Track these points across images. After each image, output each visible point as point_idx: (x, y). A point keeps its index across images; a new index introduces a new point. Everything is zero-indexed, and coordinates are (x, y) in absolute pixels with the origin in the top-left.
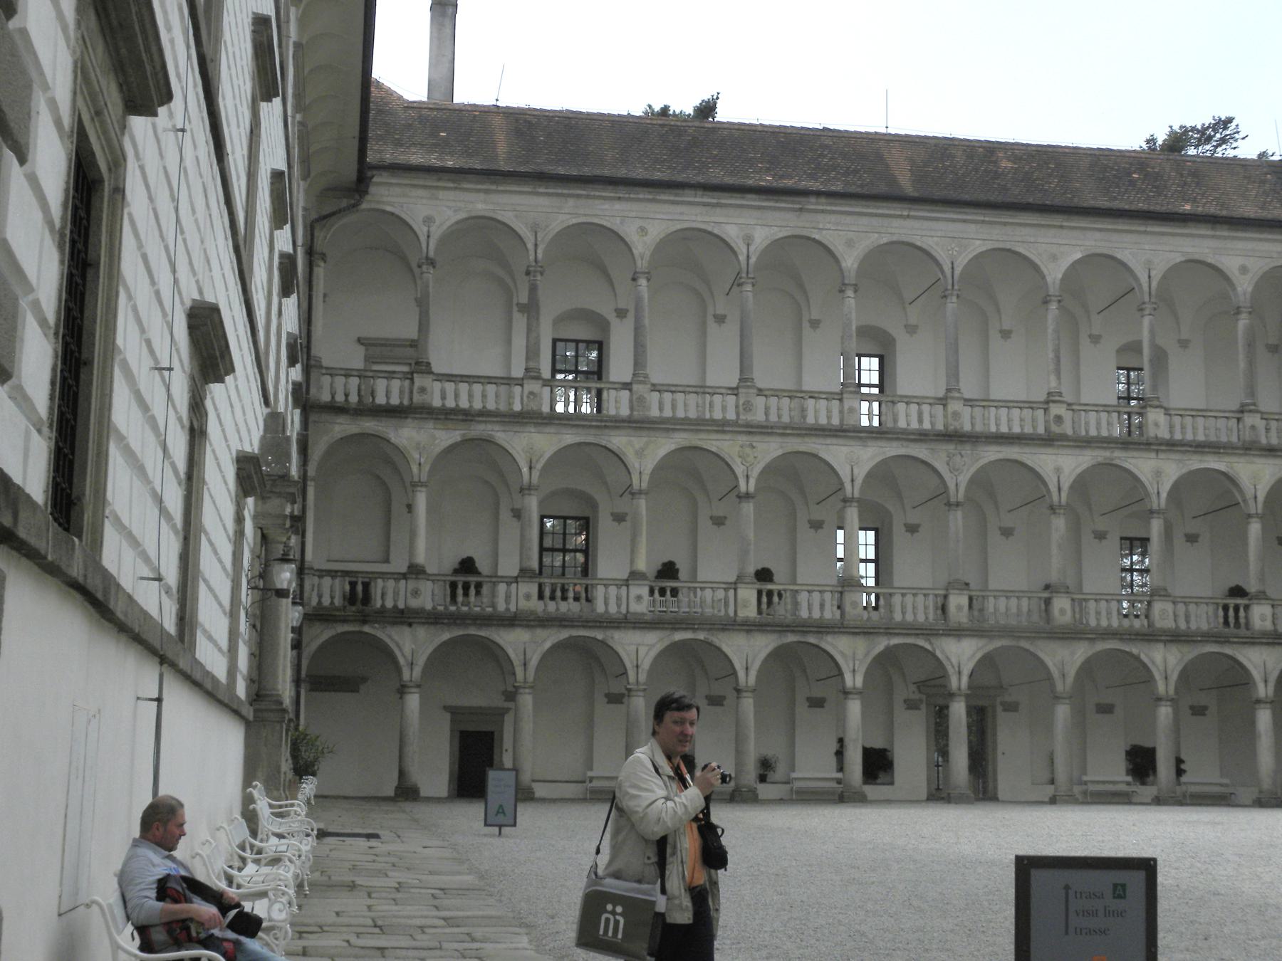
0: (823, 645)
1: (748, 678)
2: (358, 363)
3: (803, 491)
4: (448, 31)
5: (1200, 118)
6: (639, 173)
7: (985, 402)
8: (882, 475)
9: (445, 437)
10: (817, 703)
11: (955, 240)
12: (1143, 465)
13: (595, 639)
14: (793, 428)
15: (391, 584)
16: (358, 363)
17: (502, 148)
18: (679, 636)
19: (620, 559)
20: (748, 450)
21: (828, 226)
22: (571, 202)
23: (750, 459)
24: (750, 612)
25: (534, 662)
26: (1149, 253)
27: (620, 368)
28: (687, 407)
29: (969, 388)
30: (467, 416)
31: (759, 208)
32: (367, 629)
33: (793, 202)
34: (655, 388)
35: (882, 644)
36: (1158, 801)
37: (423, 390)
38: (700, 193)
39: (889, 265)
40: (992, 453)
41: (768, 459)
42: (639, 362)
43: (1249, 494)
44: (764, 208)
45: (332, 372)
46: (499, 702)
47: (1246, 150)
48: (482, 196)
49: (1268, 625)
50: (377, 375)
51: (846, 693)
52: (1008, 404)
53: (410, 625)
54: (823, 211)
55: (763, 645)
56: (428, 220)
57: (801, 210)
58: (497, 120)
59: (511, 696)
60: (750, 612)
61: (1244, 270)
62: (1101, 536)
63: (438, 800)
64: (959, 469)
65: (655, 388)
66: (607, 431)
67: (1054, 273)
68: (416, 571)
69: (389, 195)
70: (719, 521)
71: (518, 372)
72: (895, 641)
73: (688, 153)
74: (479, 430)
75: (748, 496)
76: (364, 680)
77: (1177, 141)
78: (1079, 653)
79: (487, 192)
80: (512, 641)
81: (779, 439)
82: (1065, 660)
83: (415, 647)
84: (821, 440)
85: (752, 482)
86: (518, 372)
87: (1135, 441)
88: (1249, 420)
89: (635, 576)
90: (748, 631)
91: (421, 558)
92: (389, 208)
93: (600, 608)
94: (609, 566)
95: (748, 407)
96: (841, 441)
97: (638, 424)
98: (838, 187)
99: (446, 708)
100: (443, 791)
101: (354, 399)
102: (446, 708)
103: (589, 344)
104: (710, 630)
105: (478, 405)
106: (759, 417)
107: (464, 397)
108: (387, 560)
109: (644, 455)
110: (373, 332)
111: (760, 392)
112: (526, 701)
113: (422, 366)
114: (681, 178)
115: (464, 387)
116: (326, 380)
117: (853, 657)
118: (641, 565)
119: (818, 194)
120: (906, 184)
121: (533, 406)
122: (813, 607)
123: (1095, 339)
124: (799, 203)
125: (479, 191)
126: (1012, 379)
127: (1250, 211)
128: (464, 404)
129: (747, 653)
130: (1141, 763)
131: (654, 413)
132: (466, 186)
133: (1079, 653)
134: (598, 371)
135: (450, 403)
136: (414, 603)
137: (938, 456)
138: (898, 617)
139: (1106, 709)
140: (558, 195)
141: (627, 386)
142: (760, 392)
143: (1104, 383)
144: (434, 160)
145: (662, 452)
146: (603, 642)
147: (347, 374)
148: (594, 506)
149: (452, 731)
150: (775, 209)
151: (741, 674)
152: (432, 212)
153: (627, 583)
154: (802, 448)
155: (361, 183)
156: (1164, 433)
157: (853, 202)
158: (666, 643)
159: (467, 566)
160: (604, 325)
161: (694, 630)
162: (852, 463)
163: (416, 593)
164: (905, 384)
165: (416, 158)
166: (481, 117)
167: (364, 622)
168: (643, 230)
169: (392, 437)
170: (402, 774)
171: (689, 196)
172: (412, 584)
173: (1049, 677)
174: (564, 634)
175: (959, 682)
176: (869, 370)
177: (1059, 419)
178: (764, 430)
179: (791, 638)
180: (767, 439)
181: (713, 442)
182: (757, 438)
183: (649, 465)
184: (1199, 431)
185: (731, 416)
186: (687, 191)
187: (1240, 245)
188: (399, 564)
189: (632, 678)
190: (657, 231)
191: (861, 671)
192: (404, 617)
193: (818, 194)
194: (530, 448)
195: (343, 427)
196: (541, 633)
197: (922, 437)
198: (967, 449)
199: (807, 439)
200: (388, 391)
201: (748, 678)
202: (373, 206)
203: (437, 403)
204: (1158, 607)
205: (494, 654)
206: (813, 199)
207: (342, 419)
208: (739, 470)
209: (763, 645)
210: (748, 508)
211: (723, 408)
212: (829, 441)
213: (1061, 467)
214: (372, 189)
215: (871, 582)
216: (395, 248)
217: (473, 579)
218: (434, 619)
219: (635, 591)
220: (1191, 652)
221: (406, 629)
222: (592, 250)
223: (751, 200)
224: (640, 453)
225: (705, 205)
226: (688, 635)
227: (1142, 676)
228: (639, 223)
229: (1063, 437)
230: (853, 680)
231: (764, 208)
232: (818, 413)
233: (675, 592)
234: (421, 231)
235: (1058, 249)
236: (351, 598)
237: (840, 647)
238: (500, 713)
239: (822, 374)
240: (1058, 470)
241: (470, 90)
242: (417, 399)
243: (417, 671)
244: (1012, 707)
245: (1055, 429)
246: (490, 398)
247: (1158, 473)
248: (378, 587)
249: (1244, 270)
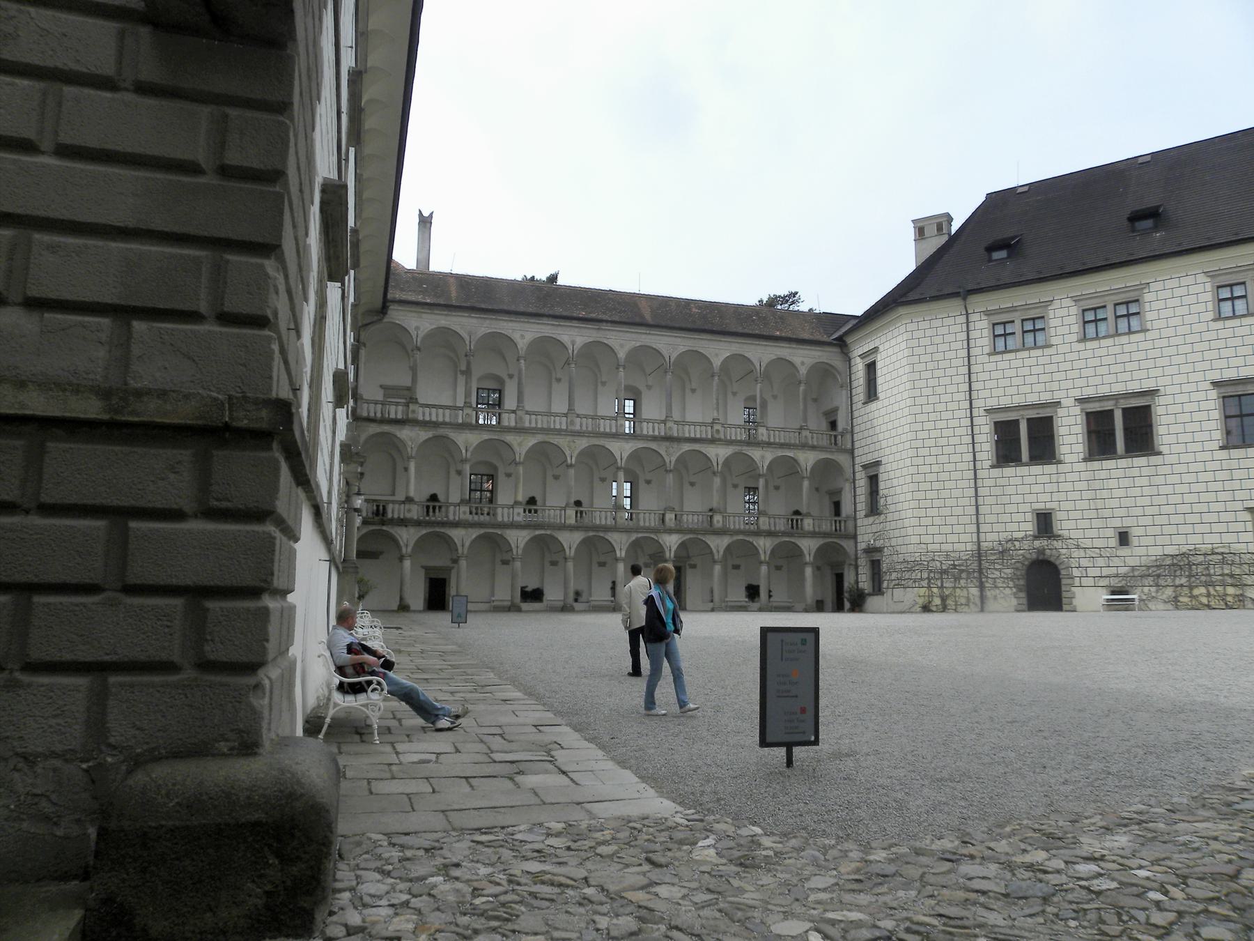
1: (570, 552)
2: (380, 397)
3: (597, 463)
5: (783, 292)
6: (521, 308)
7: (682, 423)
8: (635, 456)
9: (424, 435)
10: (602, 564)
11: (671, 345)
12: (756, 454)
15: (397, 506)
16: (380, 397)
17: (454, 294)
18: (538, 532)
19: (509, 495)
23: (572, 448)
24: (572, 521)
25: (467, 544)
26: (761, 354)
27: (510, 402)
28: (541, 422)
29: (676, 415)
30: (436, 425)
32: (384, 528)
34: (527, 413)
35: (634, 536)
36: (760, 610)
37: (414, 412)
39: (640, 357)
40: (686, 447)
42: (520, 399)
43: (804, 467)
45: (368, 402)
46: (449, 563)
47: (803, 307)
49: (811, 528)
50: (391, 403)
51: (617, 560)
52: (694, 424)
55: (578, 537)
56: (417, 328)
58: (452, 280)
59: (455, 561)
60: (572, 521)
61: (803, 363)
62: (735, 486)
63: (420, 612)
64: (671, 454)
65: (527, 413)
67: (717, 362)
68: (409, 500)
69: (397, 315)
70: (556, 477)
71: (460, 403)
72: (640, 535)
73: (545, 299)
74: (441, 431)
75: (571, 466)
76: (381, 553)
77: (773, 301)
78: (725, 541)
80: (456, 534)
82: (718, 544)
83: (407, 537)
86: (460, 403)
87: (752, 442)
88: (805, 433)
89: (517, 503)
91: (412, 494)
93: (500, 519)
94: (503, 498)
95: (572, 423)
97: (519, 430)
98: (616, 318)
100: (421, 608)
101: (379, 415)
103: (494, 391)
105: (441, 419)
106: (578, 428)
107: (434, 415)
108: (393, 494)
109: (522, 445)
111: (578, 416)
112: (463, 563)
113: (415, 401)
114: (542, 311)
115: (434, 410)
116: (365, 406)
117: (622, 544)
118: (520, 498)
119: (607, 321)
120: (648, 318)
121: (468, 420)
122: (600, 519)
123: (734, 394)
126: (696, 412)
127: (806, 336)
128: (434, 419)
129: (570, 541)
130: (753, 592)
131: (527, 425)
133: (725, 541)
134: (499, 403)
135: (427, 418)
136: (408, 516)
137: (661, 448)
138: (642, 524)
139: (736, 567)
141: (514, 412)
142: (578, 416)
143: (737, 415)
144: (420, 298)
146: (501, 535)
147: (376, 403)
148: (496, 468)
152: (419, 324)
153: (513, 507)
155: (384, 310)
156: (765, 438)
159: (434, 498)
160: (501, 381)
162: (621, 450)
163: (409, 511)
164: (646, 413)
165: (412, 298)
166: (442, 280)
169: (398, 434)
170: (401, 599)
171: (545, 321)
172: (407, 506)
173: (711, 552)
174: (482, 531)
175: (670, 554)
176: (629, 406)
177: (718, 431)
178: (580, 434)
179: (591, 534)
184: (782, 438)
185: (564, 427)
187: (802, 352)
188: (400, 496)
190: (529, 337)
191: (625, 548)
192: (403, 522)
193: (607, 321)
194: (467, 441)
195: (373, 429)
197: (655, 439)
198: (675, 445)
200: (396, 412)
203: (421, 418)
204: (762, 519)
205: (448, 541)
207: (373, 425)
208: (568, 453)
209: (578, 537)
210: (572, 471)
211: (561, 423)
213: (718, 453)
215: (628, 507)
216: (400, 341)
217: (437, 504)
218: (418, 523)
219: (516, 510)
220: (777, 541)
222: (498, 345)
223: (575, 324)
224: (520, 444)
226: (543, 532)
227: (754, 551)
229: (720, 440)
230: (621, 553)
232: (605, 426)
233: (536, 511)
234: (414, 334)
235: (718, 351)
236: (377, 513)
237: (614, 538)
238: (449, 570)
239: (608, 407)
240: (717, 455)
241: (438, 264)
242: (411, 416)
243: (409, 549)
244: (694, 566)
245: (716, 436)
246: (446, 416)
247: (763, 457)
248: (390, 508)
249: (803, 363)
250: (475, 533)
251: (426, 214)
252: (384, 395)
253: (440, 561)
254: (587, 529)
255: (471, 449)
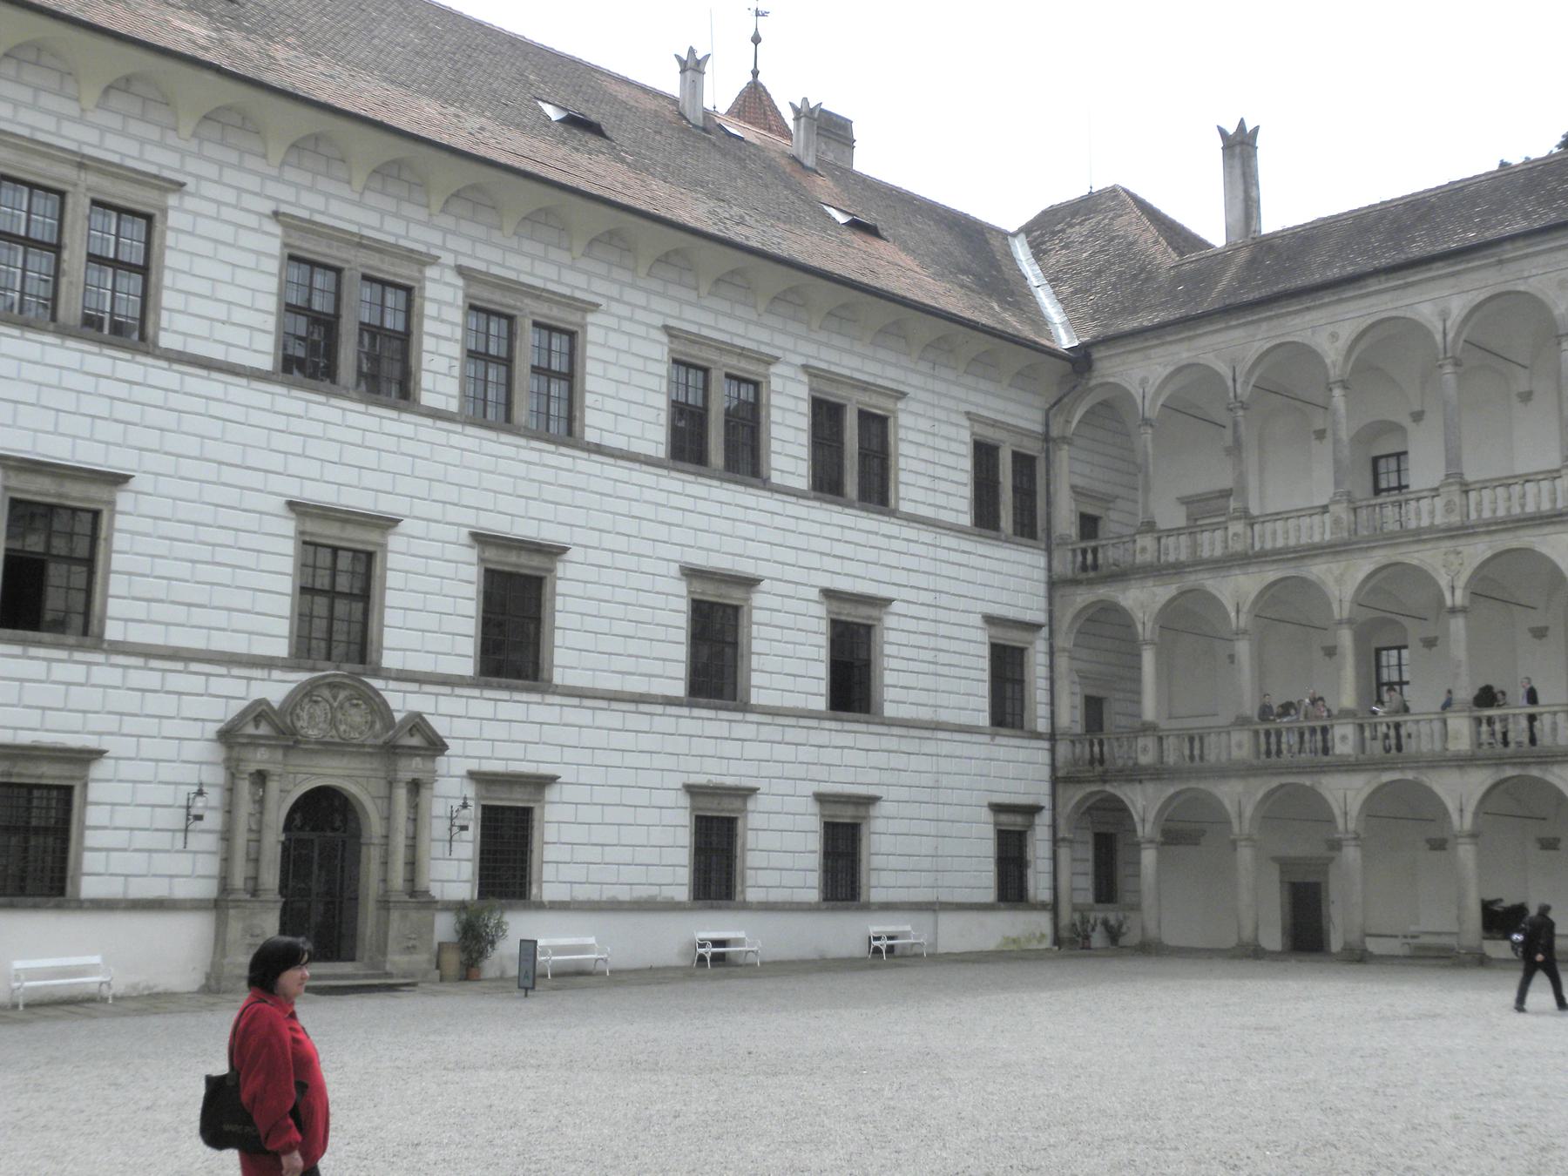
0: (1550, 778)
1: (1463, 822)
2: (1181, 521)
4: (1238, 172)
13: (1303, 786)
14: (1496, 523)
16: (1181, 521)
19: (1432, 688)
20: (1452, 557)
21: (1534, 272)
22: (1264, 326)
30: (1178, 568)
31: (1453, 274)
33: (1485, 257)
38: (1383, 278)
41: (1477, 562)
44: (1459, 272)
48: (1186, 345)
53: (1140, 782)
54: (1526, 256)
55: (1478, 781)
56: (1144, 381)
57: (1500, 262)
59: (1336, 845)
66: (1306, 561)
74: (1191, 580)
75: (1453, 611)
79: (1189, 338)
81: (1487, 538)
84: (1537, 531)
85: (1459, 593)
90: (1460, 767)
92: (1111, 380)
93: (1211, 757)
94: (1422, 698)
96: (1559, 528)
99: (1275, 859)
102: (1275, 859)
104: (1418, 768)
110: (1190, 490)
112: (1351, 854)
124: (1493, 256)
125: (1182, 340)
132: (1169, 339)
140: (1253, 322)
145: (1361, 576)
149: (1282, 882)
150: (1473, 269)
151: (1455, 817)
154: (1515, 545)
157: (1556, 235)
158: (1374, 785)
161: (1402, 769)
167: (1105, 782)
168: (1334, 336)
171: (1373, 285)
179: (1509, 772)
180: (1471, 540)
181: (1416, 556)
182: (1463, 541)
183: (1349, 591)
186: (1371, 281)
188: (1224, 719)
189: (1341, 826)
190: (1347, 332)
193: (1513, 238)
196: (1253, 782)
199: (1521, 533)
200: (1211, 544)
201: (1463, 822)
202: (1100, 380)
206: (1508, 246)
208: (1444, 582)
210: (1458, 625)
211: (1426, 514)
212: (1546, 530)
214: (1098, 365)
221: (1138, 787)
223: (1440, 269)
224: (1339, 580)
225: (1395, 288)
228: (1330, 328)
231: (1459, 272)
234: (1137, 393)
238: (1324, 865)
250: (1261, 787)
251: (1231, 130)
252: (1188, 518)
253: (1302, 847)
254: (1498, 762)
255: (1245, 608)
